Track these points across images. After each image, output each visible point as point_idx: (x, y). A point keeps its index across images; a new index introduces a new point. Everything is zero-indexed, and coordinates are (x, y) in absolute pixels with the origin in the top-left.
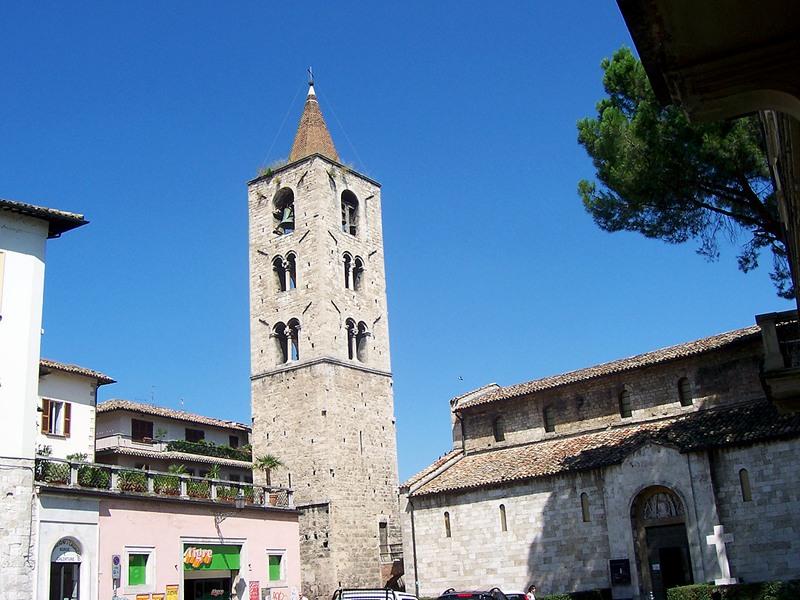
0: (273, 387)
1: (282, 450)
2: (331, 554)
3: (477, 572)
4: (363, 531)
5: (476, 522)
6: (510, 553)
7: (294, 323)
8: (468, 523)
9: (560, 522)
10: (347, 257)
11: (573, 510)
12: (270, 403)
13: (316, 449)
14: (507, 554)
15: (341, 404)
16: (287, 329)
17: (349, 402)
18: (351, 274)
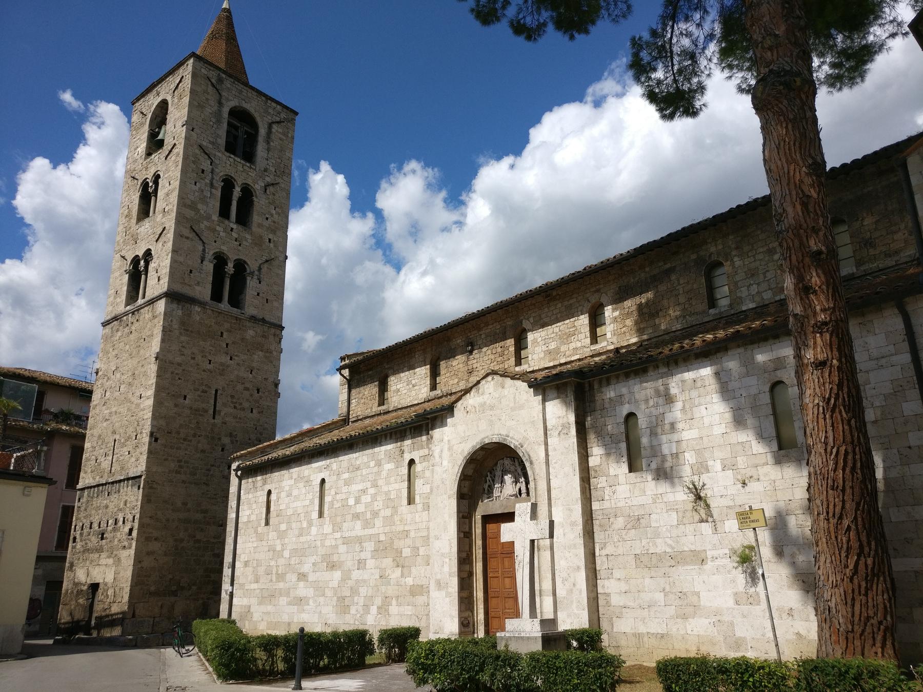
0: (119, 334)
1: (114, 409)
3: (288, 576)
4: (199, 516)
5: (295, 504)
9: (381, 507)
11: (397, 486)
13: (142, 406)
14: (322, 551)
16: (142, 263)
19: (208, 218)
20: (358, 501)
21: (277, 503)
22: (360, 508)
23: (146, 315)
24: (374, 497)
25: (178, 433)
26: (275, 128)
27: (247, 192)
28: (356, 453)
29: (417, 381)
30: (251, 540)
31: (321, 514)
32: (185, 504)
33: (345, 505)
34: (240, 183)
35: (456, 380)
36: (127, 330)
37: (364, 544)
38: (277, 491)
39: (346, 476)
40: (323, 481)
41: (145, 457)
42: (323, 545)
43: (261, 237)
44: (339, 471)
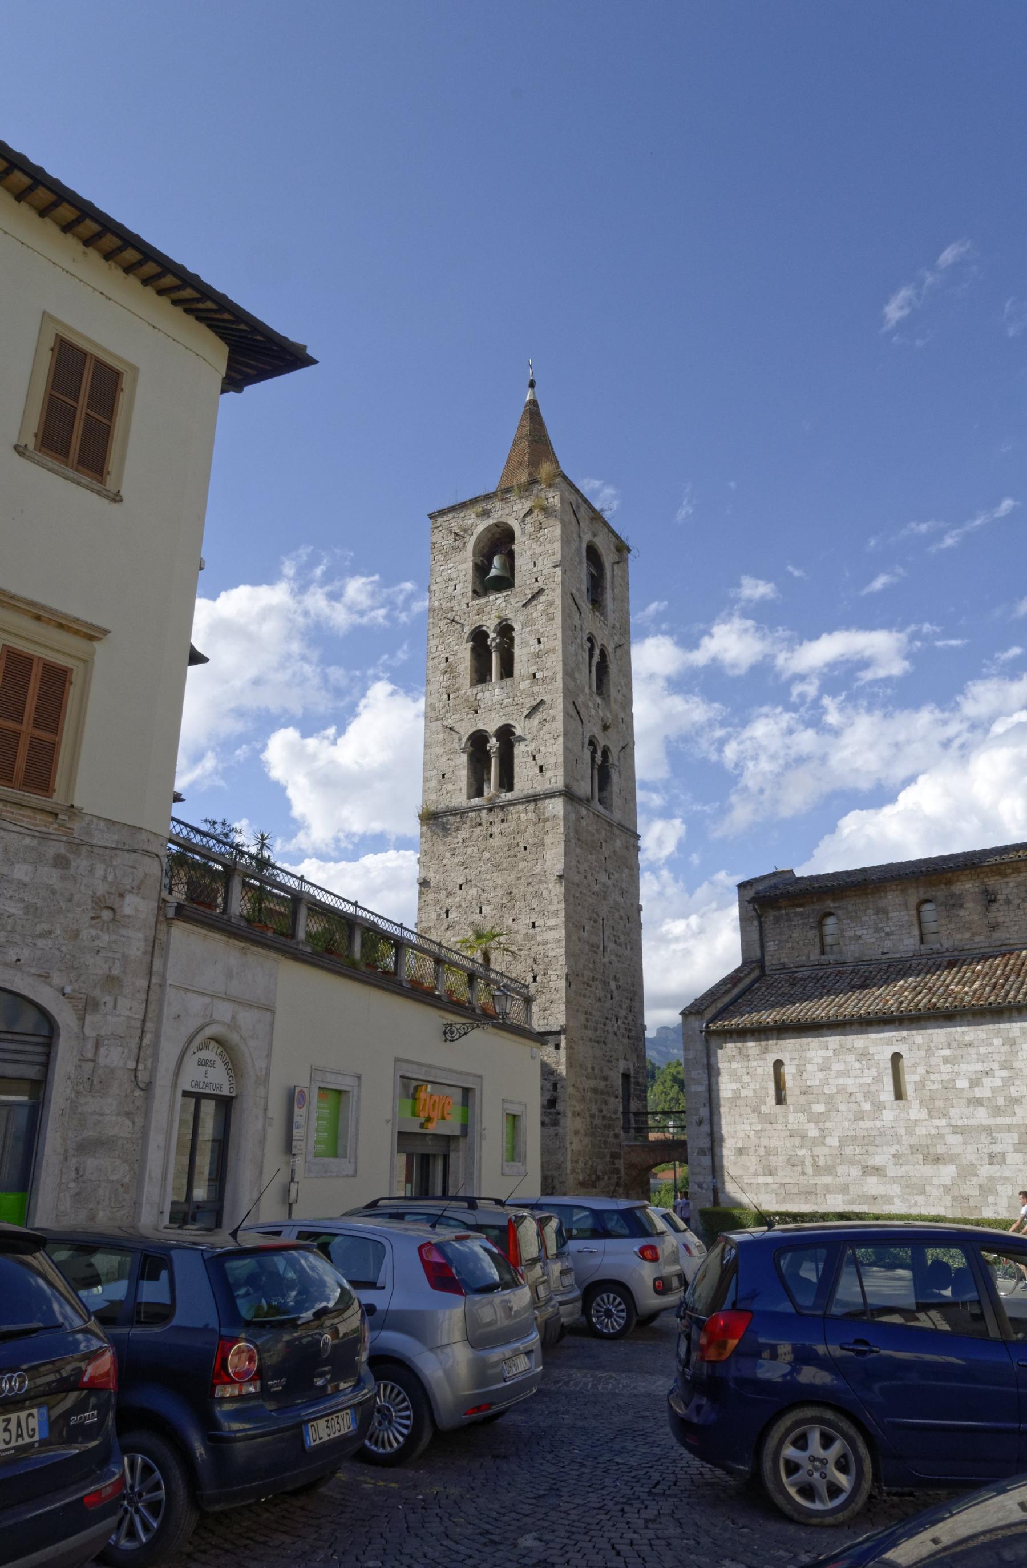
2: (562, 1121)
3: (840, 1170)
5: (841, 1081)
6: (913, 1141)
7: (506, 734)
8: (825, 1082)
10: (590, 640)
12: (456, 860)
13: (539, 939)
14: (907, 1141)
15: (581, 870)
16: (493, 742)
17: (590, 868)
18: (594, 669)
19: (583, 691)
20: (975, 1083)
21: (799, 1078)
22: (978, 1093)
23: (522, 815)
24: (1007, 1082)
25: (583, 975)
26: (615, 567)
27: (603, 654)
28: (961, 1026)
29: (893, 929)
30: (746, 1121)
31: (899, 1094)
32: (593, 1068)
33: (949, 1086)
34: (599, 644)
35: (967, 935)
36: (478, 830)
37: (998, 1135)
38: (796, 1062)
39: (947, 1052)
40: (896, 1057)
41: (563, 1007)
42: (910, 1132)
43: (617, 716)
44: (929, 1046)
